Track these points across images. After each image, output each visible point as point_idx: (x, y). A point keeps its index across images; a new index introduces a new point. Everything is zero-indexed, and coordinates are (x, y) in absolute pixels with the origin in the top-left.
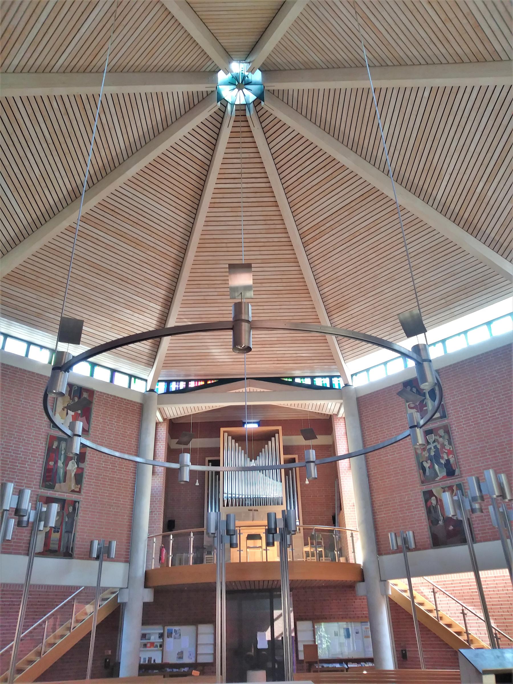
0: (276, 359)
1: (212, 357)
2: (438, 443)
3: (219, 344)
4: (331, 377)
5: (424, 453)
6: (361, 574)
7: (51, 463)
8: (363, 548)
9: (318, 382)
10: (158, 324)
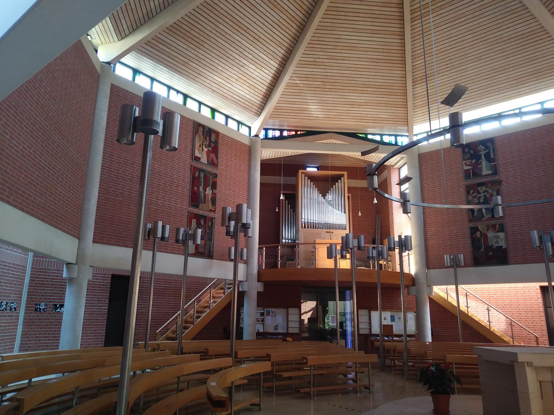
0: (359, 118)
1: (309, 112)
2: (488, 193)
3: (317, 101)
4: (396, 136)
5: (474, 200)
6: (412, 281)
7: (196, 188)
8: (416, 263)
9: (386, 139)
10: (273, 80)
